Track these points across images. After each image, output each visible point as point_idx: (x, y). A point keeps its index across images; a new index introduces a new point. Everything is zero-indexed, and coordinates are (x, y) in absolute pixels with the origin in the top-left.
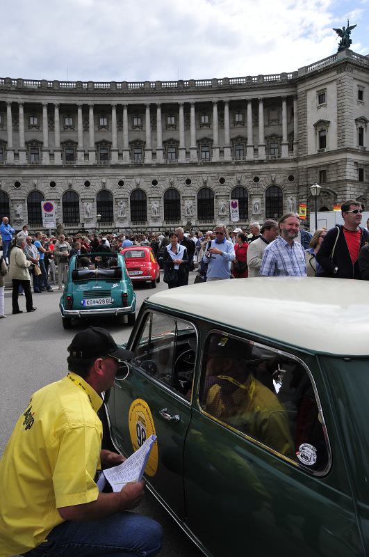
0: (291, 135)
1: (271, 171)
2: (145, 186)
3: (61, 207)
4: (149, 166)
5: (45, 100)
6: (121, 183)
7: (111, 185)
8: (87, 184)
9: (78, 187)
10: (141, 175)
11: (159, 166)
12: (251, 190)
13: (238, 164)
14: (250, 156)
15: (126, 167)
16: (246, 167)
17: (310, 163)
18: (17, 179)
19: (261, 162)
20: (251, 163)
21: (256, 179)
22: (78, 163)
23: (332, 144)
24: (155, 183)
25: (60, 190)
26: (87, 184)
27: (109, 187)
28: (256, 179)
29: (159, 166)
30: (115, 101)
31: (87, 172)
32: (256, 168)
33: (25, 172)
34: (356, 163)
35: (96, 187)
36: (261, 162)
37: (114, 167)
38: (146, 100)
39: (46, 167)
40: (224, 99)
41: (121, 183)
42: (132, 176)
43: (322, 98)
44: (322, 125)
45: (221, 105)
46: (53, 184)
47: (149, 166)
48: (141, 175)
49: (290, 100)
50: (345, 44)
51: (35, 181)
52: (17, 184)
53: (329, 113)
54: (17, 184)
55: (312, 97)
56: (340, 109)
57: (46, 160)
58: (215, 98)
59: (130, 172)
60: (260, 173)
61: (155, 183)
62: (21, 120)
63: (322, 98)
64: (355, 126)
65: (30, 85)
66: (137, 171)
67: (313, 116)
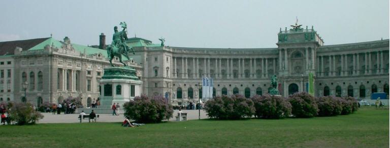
2: (377, 83)
3: (347, 91)
4: (377, 75)
5: (341, 53)
6: (368, 82)
7: (364, 83)
8: (356, 83)
9: (353, 84)
10: (375, 79)
11: (381, 75)
15: (369, 76)
18: (332, 82)
22: (353, 75)
24: (380, 82)
25: (347, 85)
26: (356, 83)
27: (364, 84)
29: (381, 75)
30: (365, 51)
31: (356, 78)
33: (335, 79)
35: (359, 84)
37: (365, 76)
38: (376, 50)
39: (341, 77)
41: (368, 82)
42: (372, 80)
46: (344, 83)
47: (377, 75)
48: (375, 79)
51: (338, 82)
52: (332, 84)
54: (332, 84)
57: (342, 74)
59: (370, 78)
61: (380, 82)
62: (334, 62)
65: (338, 49)
66: (373, 77)
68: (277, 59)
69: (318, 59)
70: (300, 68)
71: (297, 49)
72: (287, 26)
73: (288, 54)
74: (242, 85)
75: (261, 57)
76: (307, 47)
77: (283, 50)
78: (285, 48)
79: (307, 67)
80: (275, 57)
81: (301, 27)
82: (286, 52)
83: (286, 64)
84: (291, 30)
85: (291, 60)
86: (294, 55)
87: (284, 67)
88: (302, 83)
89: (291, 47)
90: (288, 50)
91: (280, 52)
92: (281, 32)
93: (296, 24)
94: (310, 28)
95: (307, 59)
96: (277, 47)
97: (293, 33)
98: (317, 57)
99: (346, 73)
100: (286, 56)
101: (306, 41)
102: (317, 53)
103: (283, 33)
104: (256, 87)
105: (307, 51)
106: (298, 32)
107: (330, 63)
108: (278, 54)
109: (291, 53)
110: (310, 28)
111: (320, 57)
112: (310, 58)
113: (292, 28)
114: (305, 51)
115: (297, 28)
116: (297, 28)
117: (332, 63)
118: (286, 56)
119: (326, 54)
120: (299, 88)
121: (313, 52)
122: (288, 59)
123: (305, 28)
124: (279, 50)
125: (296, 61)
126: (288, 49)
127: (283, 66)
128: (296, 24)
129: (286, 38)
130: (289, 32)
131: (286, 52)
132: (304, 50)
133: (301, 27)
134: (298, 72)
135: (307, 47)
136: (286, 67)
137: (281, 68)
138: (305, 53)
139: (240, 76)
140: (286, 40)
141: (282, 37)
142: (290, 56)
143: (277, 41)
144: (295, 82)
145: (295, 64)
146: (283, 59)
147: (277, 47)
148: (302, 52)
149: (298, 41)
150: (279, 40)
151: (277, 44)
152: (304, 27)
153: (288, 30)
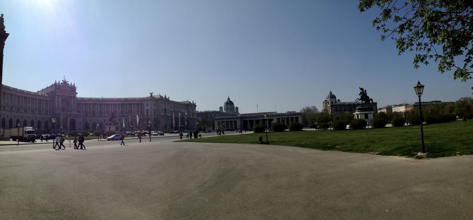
0: (141, 111)
17: (146, 117)
23: (149, 114)
43: (147, 105)
44: (147, 110)
49: (141, 104)
50: (151, 96)
53: (149, 108)
55: (145, 104)
56: (151, 107)
58: (125, 103)
63: (147, 105)
67: (146, 108)
72: (60, 80)
75: (41, 98)
76: (73, 96)
77: (59, 96)
80: (49, 99)
90: (62, 96)
92: (56, 83)
94: (73, 84)
99: (92, 114)
104: (38, 119)
110: (73, 84)
115: (65, 82)
116: (65, 82)
119: (79, 102)
123: (70, 84)
132: (71, 97)
133: (68, 83)
144: (74, 118)
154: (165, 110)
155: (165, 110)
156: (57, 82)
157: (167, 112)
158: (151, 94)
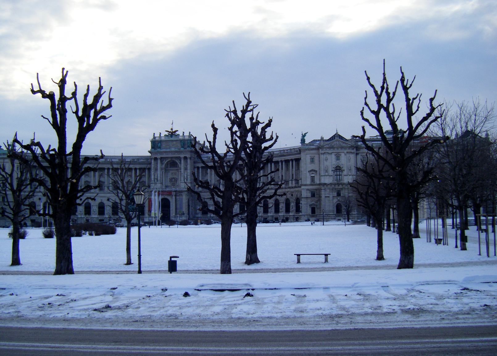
1: (296, 191)
12: (291, 200)
13: (286, 188)
14: (290, 185)
16: (289, 190)
19: (292, 188)
20: (290, 188)
21: (292, 195)
28: (292, 195)
32: (292, 190)
34: (307, 190)
36: (292, 188)
40: (283, 160)
45: (282, 162)
50: (303, 141)
60: (293, 192)
64: (308, 174)
68: (149, 169)
69: (196, 170)
70: (176, 180)
71: (172, 158)
73: (162, 164)
74: (108, 200)
75: (131, 166)
76: (182, 156)
77: (156, 159)
78: (159, 156)
79: (182, 179)
81: (177, 133)
82: (159, 161)
83: (159, 176)
84: (166, 135)
85: (166, 170)
86: (169, 166)
87: (157, 179)
88: (174, 197)
89: (164, 156)
91: (153, 161)
92: (154, 137)
93: (172, 129)
94: (187, 134)
95: (182, 170)
96: (149, 154)
97: (167, 139)
98: (195, 167)
100: (159, 165)
101: (182, 149)
102: (195, 163)
103: (157, 139)
105: (182, 161)
106: (174, 138)
107: (209, 174)
108: (150, 164)
109: (165, 162)
111: (198, 168)
112: (186, 169)
113: (167, 133)
114: (181, 161)
115: (172, 134)
116: (172, 134)
117: (211, 174)
118: (159, 165)
120: (171, 204)
121: (189, 161)
122: (162, 169)
123: (181, 135)
124: (151, 159)
125: (171, 172)
126: (161, 158)
127: (156, 177)
128: (172, 129)
129: (159, 145)
130: (163, 139)
131: (159, 161)
132: (179, 158)
134: (174, 185)
135: (182, 156)
136: (159, 178)
137: (153, 179)
138: (181, 163)
139: (106, 188)
140: (160, 148)
141: (156, 144)
142: (164, 166)
143: (149, 148)
144: (166, 197)
145: (170, 176)
146: (156, 170)
147: (149, 154)
148: (177, 161)
149: (173, 149)
150: (153, 147)
151: (149, 152)
152: (180, 133)
153: (162, 135)
154: (338, 169)
155: (338, 169)
156: (157, 135)
157: (345, 173)
158: (304, 136)
